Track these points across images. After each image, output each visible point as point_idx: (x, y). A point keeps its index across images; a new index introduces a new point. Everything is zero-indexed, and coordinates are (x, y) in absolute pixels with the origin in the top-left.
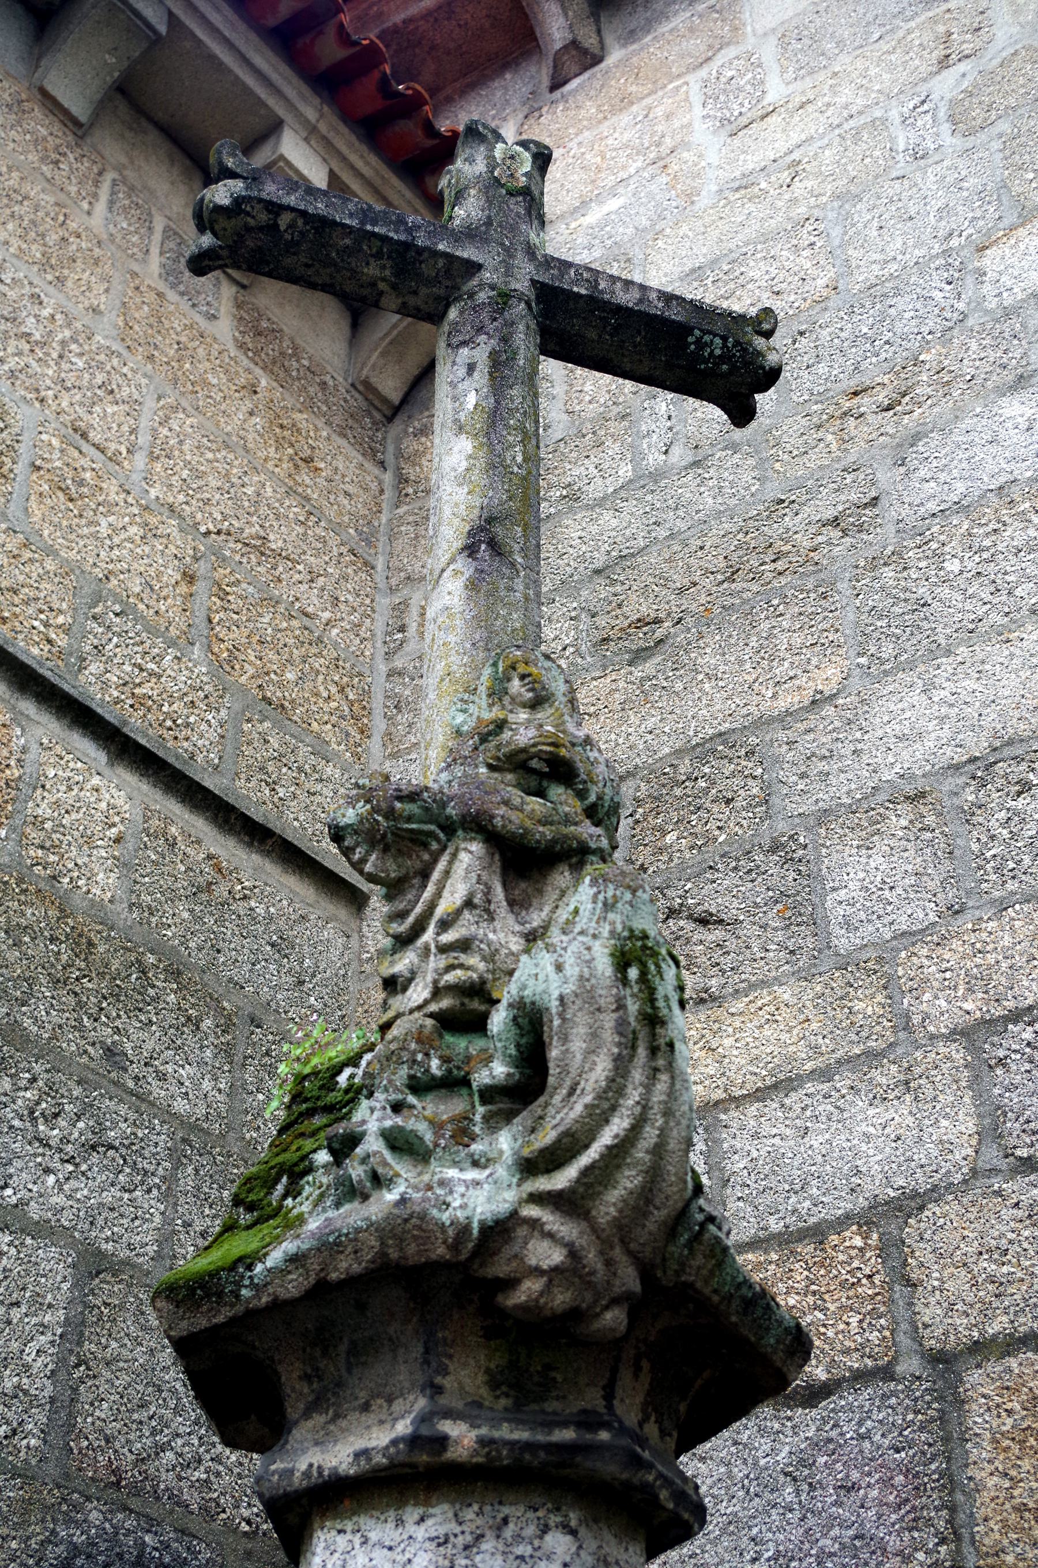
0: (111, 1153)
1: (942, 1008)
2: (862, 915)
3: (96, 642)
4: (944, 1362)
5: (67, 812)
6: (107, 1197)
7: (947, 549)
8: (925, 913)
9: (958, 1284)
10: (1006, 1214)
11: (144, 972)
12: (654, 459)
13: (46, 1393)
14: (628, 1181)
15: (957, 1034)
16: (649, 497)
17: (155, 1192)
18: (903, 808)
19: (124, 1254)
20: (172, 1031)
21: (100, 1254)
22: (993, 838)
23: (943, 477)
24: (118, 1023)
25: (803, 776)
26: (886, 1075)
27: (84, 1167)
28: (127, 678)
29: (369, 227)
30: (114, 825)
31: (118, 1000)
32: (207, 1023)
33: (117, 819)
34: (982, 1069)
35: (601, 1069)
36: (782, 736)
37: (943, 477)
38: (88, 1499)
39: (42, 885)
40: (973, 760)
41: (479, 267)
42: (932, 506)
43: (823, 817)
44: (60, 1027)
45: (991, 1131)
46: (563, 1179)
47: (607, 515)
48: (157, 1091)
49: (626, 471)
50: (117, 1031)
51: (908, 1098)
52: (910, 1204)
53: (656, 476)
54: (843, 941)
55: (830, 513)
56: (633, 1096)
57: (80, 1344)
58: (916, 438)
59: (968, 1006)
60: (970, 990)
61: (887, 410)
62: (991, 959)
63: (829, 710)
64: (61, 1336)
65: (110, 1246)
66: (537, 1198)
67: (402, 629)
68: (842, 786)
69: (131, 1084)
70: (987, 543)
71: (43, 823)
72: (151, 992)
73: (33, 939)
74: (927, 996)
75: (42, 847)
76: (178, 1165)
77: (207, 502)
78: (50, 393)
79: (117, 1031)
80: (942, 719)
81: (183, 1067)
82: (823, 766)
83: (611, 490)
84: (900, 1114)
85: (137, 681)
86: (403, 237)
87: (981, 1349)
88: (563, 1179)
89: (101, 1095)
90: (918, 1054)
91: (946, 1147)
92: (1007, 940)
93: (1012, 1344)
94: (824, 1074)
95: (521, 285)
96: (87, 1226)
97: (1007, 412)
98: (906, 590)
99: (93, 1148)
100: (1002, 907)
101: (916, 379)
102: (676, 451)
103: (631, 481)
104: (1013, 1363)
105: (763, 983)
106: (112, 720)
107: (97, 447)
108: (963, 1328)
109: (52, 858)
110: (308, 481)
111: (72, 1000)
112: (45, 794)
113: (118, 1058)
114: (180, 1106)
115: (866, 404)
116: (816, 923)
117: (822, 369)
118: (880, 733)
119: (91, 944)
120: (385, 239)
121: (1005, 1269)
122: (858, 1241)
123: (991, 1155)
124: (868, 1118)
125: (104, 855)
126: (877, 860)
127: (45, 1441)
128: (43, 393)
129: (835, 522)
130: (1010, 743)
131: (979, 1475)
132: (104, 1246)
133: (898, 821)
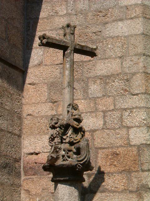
1: (101, 107)
2: (93, 93)
4: (96, 148)
7: (109, 43)
8: (100, 95)
9: (99, 141)
10: (105, 134)
12: (70, 11)
14: (87, 163)
15: (102, 111)
16: (69, 18)
18: (99, 80)
19: (4, 129)
22: (109, 87)
23: (110, 31)
25: (87, 71)
26: (94, 115)
32: (10, 96)
34: (104, 117)
35: (85, 155)
36: (85, 64)
37: (110, 31)
40: (108, 76)
42: (108, 36)
43: (88, 78)
45: (104, 124)
46: (82, 163)
47: (62, 19)
48: (6, 107)
49: (65, 12)
50: (2, 100)
51: (96, 118)
52: (94, 131)
53: (70, 14)
54: (90, 97)
55: (94, 31)
56: (87, 157)
58: (107, 23)
59: (104, 108)
60: (104, 106)
61: (104, 17)
62: (107, 103)
63: (91, 62)
66: (79, 163)
67: (29, 27)
68: (91, 75)
70: (114, 44)
74: (99, 106)
76: (8, 116)
77: (7, 14)
79: (2, 100)
80: (106, 69)
82: (90, 71)
83: (63, 14)
84: (95, 120)
87: (100, 148)
88: (82, 163)
90: (98, 113)
91: (100, 125)
92: (109, 101)
93: (104, 148)
94: (87, 113)
97: (120, 24)
98: (103, 47)
100: (109, 96)
101: (108, 13)
102: (73, 11)
103: (66, 14)
104: (104, 150)
105: (80, 99)
108: (99, 146)
110: (17, 3)
114: (8, 108)
115: (101, 14)
116: (87, 93)
117: (95, 6)
118: (97, 68)
121: (104, 140)
122: (89, 134)
123: (104, 127)
124: (91, 120)
126: (95, 86)
129: (95, 33)
130: (113, 75)
131: (98, 161)
133: (98, 82)
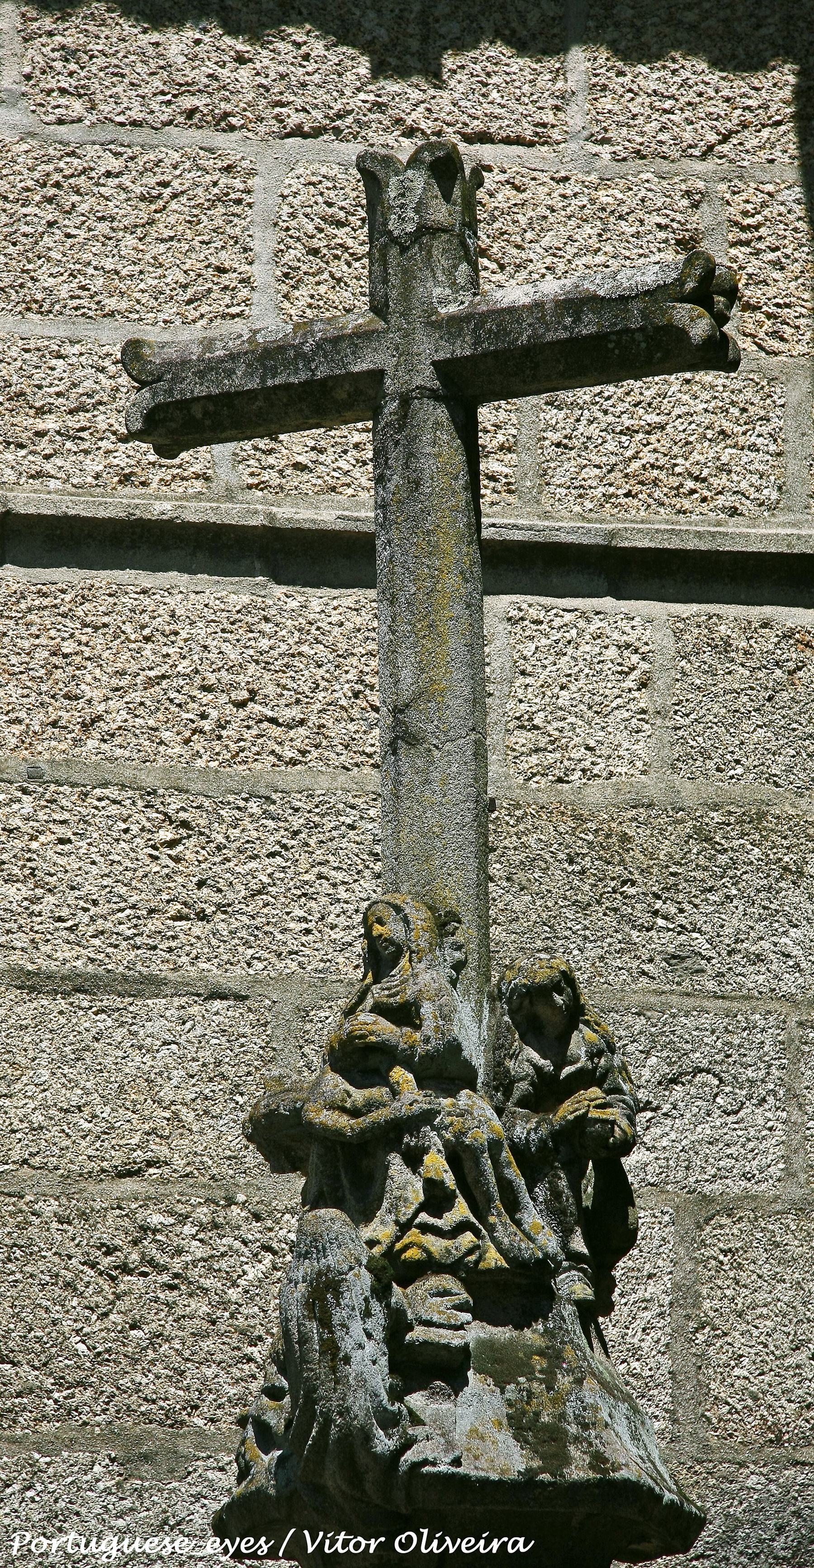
0: (699, 1078)
3: (556, 437)
5: (562, 688)
6: (705, 1130)
11: (707, 840)
13: (664, 1370)
17: (771, 1099)
20: (762, 895)
21: (706, 1199)
24: (681, 920)
27: (666, 1108)
28: (613, 459)
29: (270, 383)
30: (633, 669)
31: (678, 891)
33: (635, 658)
38: (742, 1465)
39: (543, 799)
41: (378, 375)
44: (602, 958)
57: (697, 1305)
64: (671, 1304)
65: (717, 1187)
69: (711, 985)
71: (530, 719)
72: (723, 859)
73: (545, 870)
75: (537, 750)
78: (421, 109)
81: (785, 933)
85: (629, 453)
86: (303, 376)
89: (674, 1016)
95: (426, 377)
96: (681, 1174)
99: (674, 1081)
106: (593, 541)
107: (507, 141)
109: (551, 757)
111: (611, 921)
112: (529, 680)
113: (688, 963)
119: (625, 838)
120: (288, 387)
125: (627, 715)
127: (675, 1421)
128: (409, 122)
132: (707, 1188)
